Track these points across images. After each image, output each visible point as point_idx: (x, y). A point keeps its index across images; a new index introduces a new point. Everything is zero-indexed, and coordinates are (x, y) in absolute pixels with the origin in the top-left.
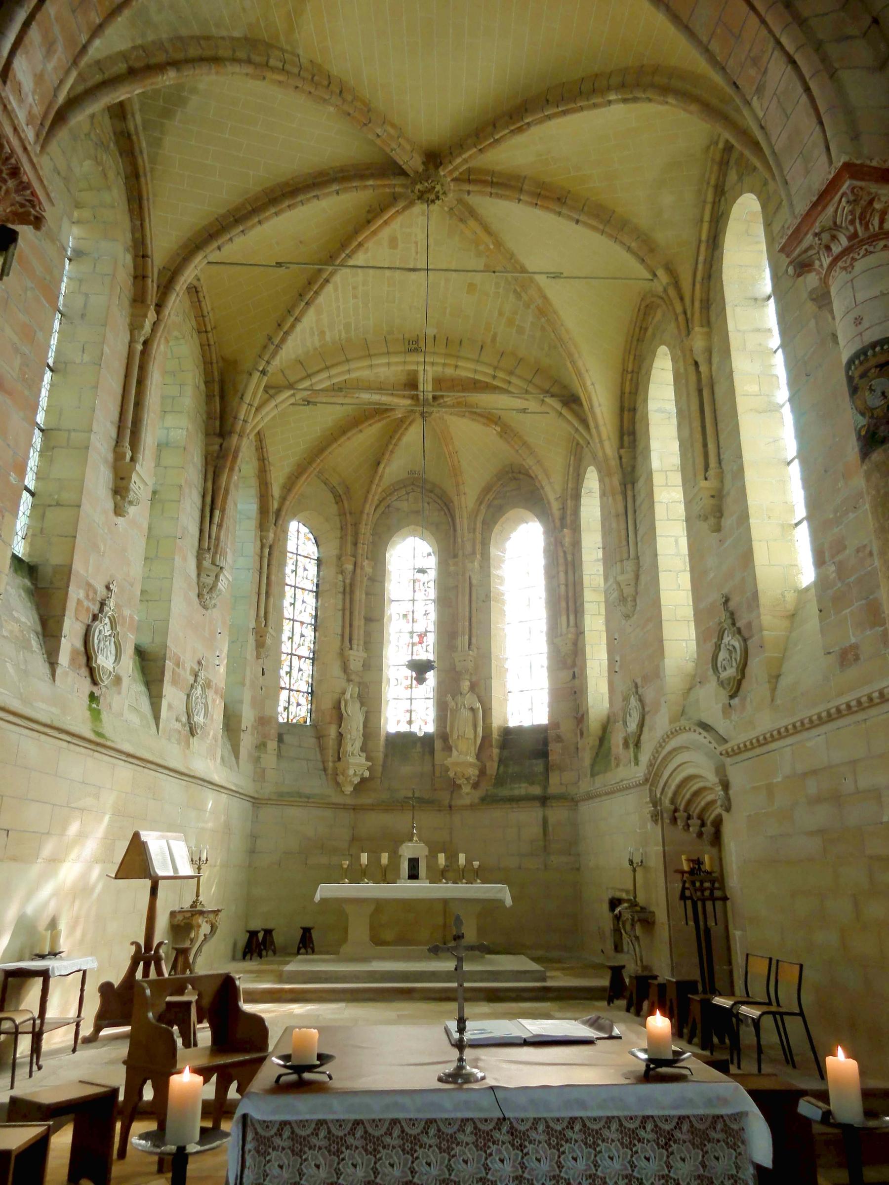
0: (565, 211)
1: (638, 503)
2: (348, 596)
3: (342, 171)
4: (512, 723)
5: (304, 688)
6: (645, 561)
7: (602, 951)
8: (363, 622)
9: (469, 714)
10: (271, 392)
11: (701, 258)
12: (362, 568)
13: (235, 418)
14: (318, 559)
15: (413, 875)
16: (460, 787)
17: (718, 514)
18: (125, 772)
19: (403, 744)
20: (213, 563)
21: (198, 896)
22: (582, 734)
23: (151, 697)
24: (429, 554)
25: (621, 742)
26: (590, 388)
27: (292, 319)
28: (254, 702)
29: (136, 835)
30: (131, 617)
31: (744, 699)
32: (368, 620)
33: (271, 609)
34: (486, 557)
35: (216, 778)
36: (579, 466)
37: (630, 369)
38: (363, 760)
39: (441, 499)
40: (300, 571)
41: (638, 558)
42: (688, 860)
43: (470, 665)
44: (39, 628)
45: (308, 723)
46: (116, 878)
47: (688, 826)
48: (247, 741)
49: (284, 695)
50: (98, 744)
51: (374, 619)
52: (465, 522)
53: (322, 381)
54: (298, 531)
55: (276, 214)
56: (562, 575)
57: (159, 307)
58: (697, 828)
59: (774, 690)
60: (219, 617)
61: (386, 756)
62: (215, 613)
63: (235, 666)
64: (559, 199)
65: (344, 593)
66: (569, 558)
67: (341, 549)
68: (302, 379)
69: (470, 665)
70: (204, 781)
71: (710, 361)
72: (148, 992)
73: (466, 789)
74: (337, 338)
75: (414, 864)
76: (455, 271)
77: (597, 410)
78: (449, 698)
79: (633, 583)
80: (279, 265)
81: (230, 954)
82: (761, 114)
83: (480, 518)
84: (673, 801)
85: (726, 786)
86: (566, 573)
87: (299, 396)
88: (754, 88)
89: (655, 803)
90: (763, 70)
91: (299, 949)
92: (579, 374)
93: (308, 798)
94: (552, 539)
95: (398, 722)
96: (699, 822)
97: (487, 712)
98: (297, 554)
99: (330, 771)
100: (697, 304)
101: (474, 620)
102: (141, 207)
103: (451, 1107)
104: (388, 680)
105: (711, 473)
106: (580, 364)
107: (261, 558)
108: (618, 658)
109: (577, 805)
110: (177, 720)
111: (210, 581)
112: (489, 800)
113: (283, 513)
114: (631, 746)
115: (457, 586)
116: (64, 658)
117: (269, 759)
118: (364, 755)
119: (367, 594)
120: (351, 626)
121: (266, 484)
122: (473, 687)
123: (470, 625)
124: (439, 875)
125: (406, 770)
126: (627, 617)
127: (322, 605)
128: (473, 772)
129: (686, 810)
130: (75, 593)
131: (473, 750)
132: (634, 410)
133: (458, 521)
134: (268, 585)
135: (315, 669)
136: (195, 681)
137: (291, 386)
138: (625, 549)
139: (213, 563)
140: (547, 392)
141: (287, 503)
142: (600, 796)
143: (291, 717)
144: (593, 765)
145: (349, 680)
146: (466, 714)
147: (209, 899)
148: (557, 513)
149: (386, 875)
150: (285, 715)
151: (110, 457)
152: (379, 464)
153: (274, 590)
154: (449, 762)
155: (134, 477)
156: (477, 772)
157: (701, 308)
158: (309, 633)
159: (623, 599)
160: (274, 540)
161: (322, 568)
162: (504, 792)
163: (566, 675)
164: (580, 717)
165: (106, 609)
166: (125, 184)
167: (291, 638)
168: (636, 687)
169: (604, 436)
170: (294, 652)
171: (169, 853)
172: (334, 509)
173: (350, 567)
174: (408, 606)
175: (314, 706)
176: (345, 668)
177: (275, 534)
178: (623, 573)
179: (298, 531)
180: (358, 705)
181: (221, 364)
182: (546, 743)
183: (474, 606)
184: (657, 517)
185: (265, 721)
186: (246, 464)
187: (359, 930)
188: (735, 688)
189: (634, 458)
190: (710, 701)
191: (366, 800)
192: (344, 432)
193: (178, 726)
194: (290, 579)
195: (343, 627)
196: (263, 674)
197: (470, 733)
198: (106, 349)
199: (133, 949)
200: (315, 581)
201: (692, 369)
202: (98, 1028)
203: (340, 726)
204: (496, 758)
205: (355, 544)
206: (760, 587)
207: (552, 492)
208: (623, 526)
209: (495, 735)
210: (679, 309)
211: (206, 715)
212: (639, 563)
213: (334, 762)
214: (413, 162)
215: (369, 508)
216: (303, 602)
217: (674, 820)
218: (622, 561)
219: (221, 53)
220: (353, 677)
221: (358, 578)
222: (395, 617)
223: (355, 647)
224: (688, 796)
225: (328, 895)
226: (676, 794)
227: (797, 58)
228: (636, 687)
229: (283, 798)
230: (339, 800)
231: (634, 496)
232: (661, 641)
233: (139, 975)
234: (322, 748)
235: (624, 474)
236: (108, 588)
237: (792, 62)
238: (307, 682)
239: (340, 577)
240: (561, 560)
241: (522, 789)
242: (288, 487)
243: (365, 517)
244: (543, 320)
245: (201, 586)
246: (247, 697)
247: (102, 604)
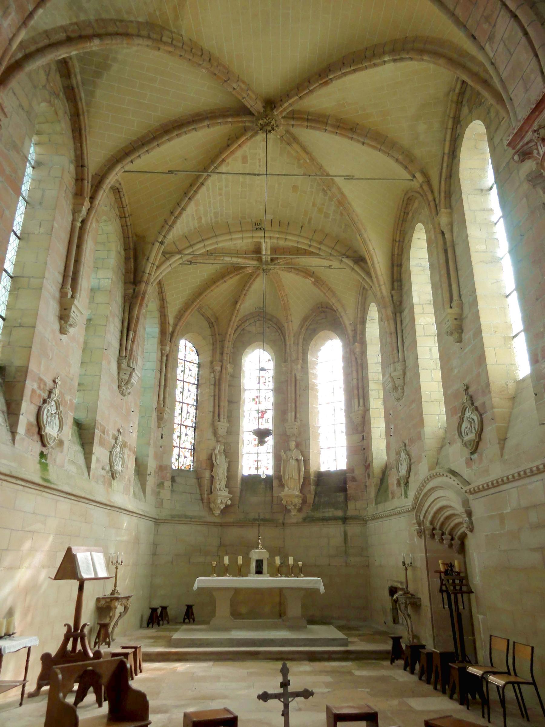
0: (355, 136)
1: (404, 325)
2: (217, 387)
3: (211, 113)
4: (323, 469)
5: (189, 446)
6: (410, 363)
7: (385, 623)
8: (226, 404)
10: (167, 256)
11: (445, 165)
12: (226, 369)
13: (144, 272)
14: (199, 364)
15: (259, 572)
16: (289, 511)
17: (460, 331)
18: (65, 505)
19: (252, 482)
20: (128, 366)
21: (115, 586)
22: (369, 475)
23: (85, 454)
24: (269, 360)
25: (395, 482)
26: (372, 251)
27: (180, 209)
28: (157, 456)
29: (69, 550)
30: (71, 401)
31: (481, 455)
32: (230, 402)
33: (167, 395)
34: (305, 361)
35: (130, 507)
36: (365, 303)
37: (398, 240)
38: (226, 493)
39: (276, 325)
40: (187, 371)
41: (405, 361)
42: (444, 564)
44: (5, 409)
45: (192, 469)
46: (55, 579)
47: (442, 540)
48: (151, 481)
49: (176, 451)
50: (45, 486)
51: (234, 402)
52: (292, 339)
53: (200, 249)
54: (186, 346)
55: (169, 140)
56: (354, 373)
57: (92, 199)
58: (449, 541)
59: (502, 448)
61: (242, 490)
62: (130, 399)
63: (143, 432)
64: (351, 129)
65: (215, 385)
66: (359, 361)
67: (213, 357)
68: (186, 248)
70: (120, 508)
71: (452, 231)
72: (60, 676)
73: (294, 512)
74: (210, 222)
75: (259, 563)
76: (284, 175)
77: (377, 266)
78: (282, 452)
79: (402, 377)
80: (170, 172)
81: (138, 624)
82: (491, 55)
83: (301, 337)
84: (432, 523)
85: (469, 514)
86: (357, 371)
87: (186, 258)
88: (487, 37)
90: (493, 24)
91: (184, 619)
92: (365, 243)
93: (191, 518)
94: (348, 350)
95: (250, 468)
96: (450, 537)
97: (307, 461)
98: (185, 361)
99: (205, 501)
100: (443, 194)
101: (298, 402)
102: (80, 135)
104: (243, 441)
105: (454, 304)
106: (365, 236)
107: (161, 363)
108: (392, 427)
109: (366, 523)
110: (103, 469)
112: (308, 520)
113: (176, 334)
114: (402, 485)
115: (287, 381)
116: (21, 429)
117: (166, 493)
118: (227, 490)
119: (229, 386)
120: (219, 406)
121: (165, 315)
122: (298, 446)
123: (296, 405)
125: (254, 499)
126: (398, 399)
127: (201, 393)
129: (441, 528)
130: (30, 385)
131: (298, 487)
132: (400, 266)
133: (287, 339)
134: (166, 380)
135: (196, 434)
136: (116, 443)
137: (179, 252)
138: (396, 355)
139: (128, 366)
140: (344, 255)
141: (178, 327)
142: (382, 517)
143: (180, 465)
144: (376, 497)
145: (218, 441)
146: (293, 463)
147: (123, 590)
149: (241, 572)
150: (176, 464)
151: (57, 295)
152: (237, 302)
153: (169, 383)
154: (282, 494)
155: (73, 309)
156: (301, 501)
157: (445, 197)
158: (193, 411)
159: (395, 388)
160: (170, 351)
161: (201, 369)
162: (318, 515)
164: (367, 465)
165: (53, 395)
166: (71, 120)
167: (181, 414)
168: (405, 446)
169: (382, 283)
170: (182, 423)
171: (92, 563)
172: (208, 332)
173: (218, 368)
174: (255, 393)
175: (195, 458)
176: (215, 433)
177: (170, 348)
178: (395, 370)
179: (186, 346)
180: (223, 457)
181: (135, 238)
182: (345, 482)
183: (298, 392)
184: (417, 335)
185: (163, 468)
187: (223, 609)
188: (475, 447)
189: (401, 296)
190: (457, 455)
191: (230, 519)
192: (215, 282)
193: (103, 473)
194: (180, 376)
195: (214, 406)
196: (162, 437)
197: (295, 476)
198: (55, 225)
199: (65, 630)
200: (196, 378)
201: (440, 236)
202: (39, 686)
203: (212, 471)
204: (313, 492)
205: (222, 354)
206: (491, 379)
207: (347, 319)
208: (394, 340)
209: (312, 477)
210: (430, 198)
211: (123, 465)
212: (405, 364)
213: (208, 495)
214: (257, 106)
215: (231, 331)
216: (189, 391)
217: (433, 536)
218: (394, 363)
219: (130, 31)
220: (220, 439)
221: (224, 376)
222: (247, 400)
223: (221, 420)
224: (442, 519)
225: (203, 585)
226: (434, 517)
227: (518, 13)
228: (405, 446)
230: (213, 519)
231: (401, 321)
232: (421, 415)
233: (69, 647)
234: (200, 486)
235: (394, 307)
236: (54, 381)
237: (515, 17)
238: (191, 443)
239: (212, 375)
240: (354, 363)
241: (330, 512)
242: (179, 317)
243: (228, 336)
244: (341, 208)
245: (120, 380)
246: (151, 452)
247: (50, 392)
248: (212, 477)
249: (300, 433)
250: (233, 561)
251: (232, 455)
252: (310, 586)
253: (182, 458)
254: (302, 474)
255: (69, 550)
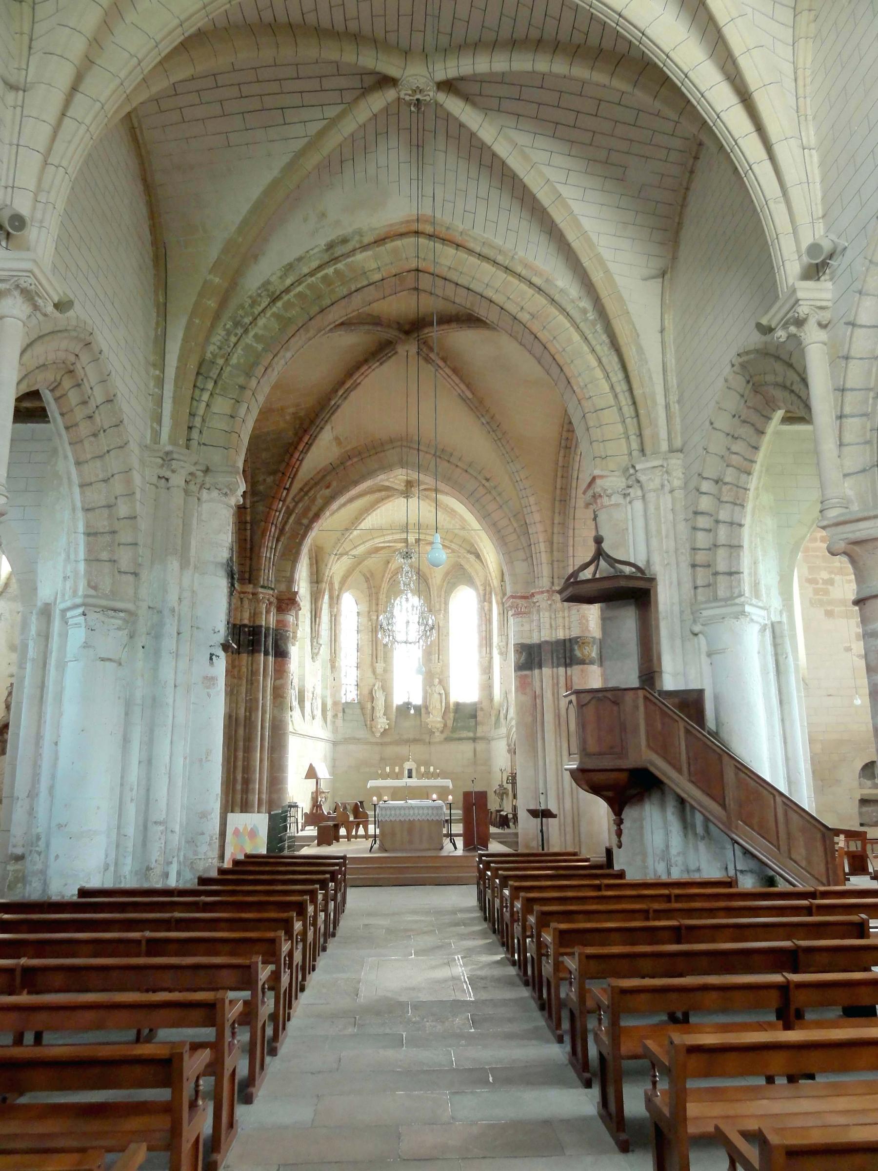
9: (439, 696)
15: (410, 777)
29: (311, 765)
33: (337, 649)
43: (438, 670)
48: (329, 715)
60: (318, 663)
69: (438, 670)
75: (410, 771)
83: (444, 589)
89: (509, 745)
97: (447, 695)
103: (406, 805)
106: (481, 545)
111: (316, 651)
112: (448, 740)
117: (339, 722)
122: (440, 682)
124: (421, 776)
125: (407, 724)
128: (440, 726)
131: (441, 714)
137: (346, 553)
146: (436, 696)
148: (482, 592)
149: (398, 776)
162: (456, 736)
163: (486, 677)
164: (491, 699)
172: (366, 585)
176: (374, 672)
182: (476, 711)
186: (325, 586)
191: (387, 739)
214: (402, 487)
215: (385, 586)
225: (374, 785)
229: (348, 740)
234: (364, 714)
240: (484, 618)
242: (343, 582)
246: (328, 693)
248: (373, 708)
249: (442, 672)
250: (392, 770)
251: (387, 689)
252: (444, 784)
253: (350, 694)
254: (444, 704)
255: (311, 765)
